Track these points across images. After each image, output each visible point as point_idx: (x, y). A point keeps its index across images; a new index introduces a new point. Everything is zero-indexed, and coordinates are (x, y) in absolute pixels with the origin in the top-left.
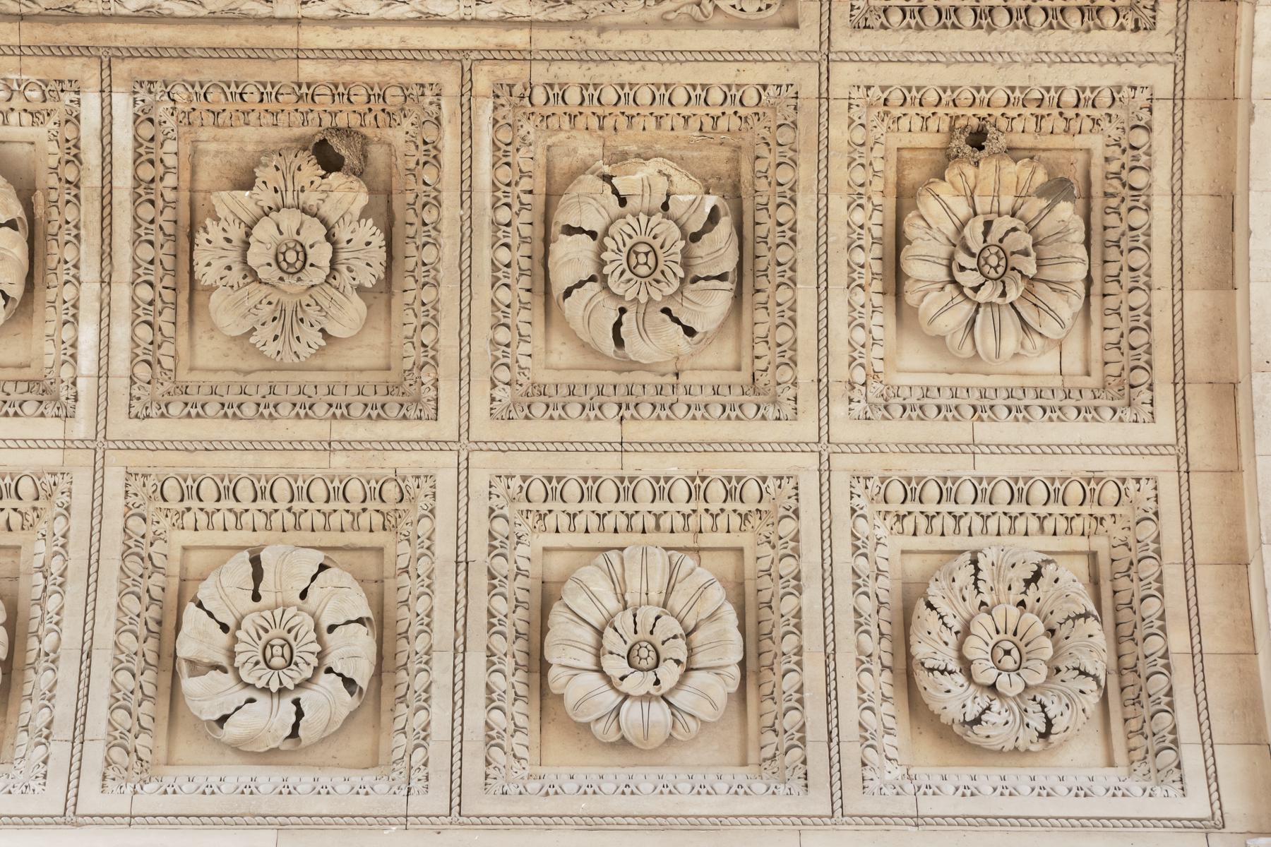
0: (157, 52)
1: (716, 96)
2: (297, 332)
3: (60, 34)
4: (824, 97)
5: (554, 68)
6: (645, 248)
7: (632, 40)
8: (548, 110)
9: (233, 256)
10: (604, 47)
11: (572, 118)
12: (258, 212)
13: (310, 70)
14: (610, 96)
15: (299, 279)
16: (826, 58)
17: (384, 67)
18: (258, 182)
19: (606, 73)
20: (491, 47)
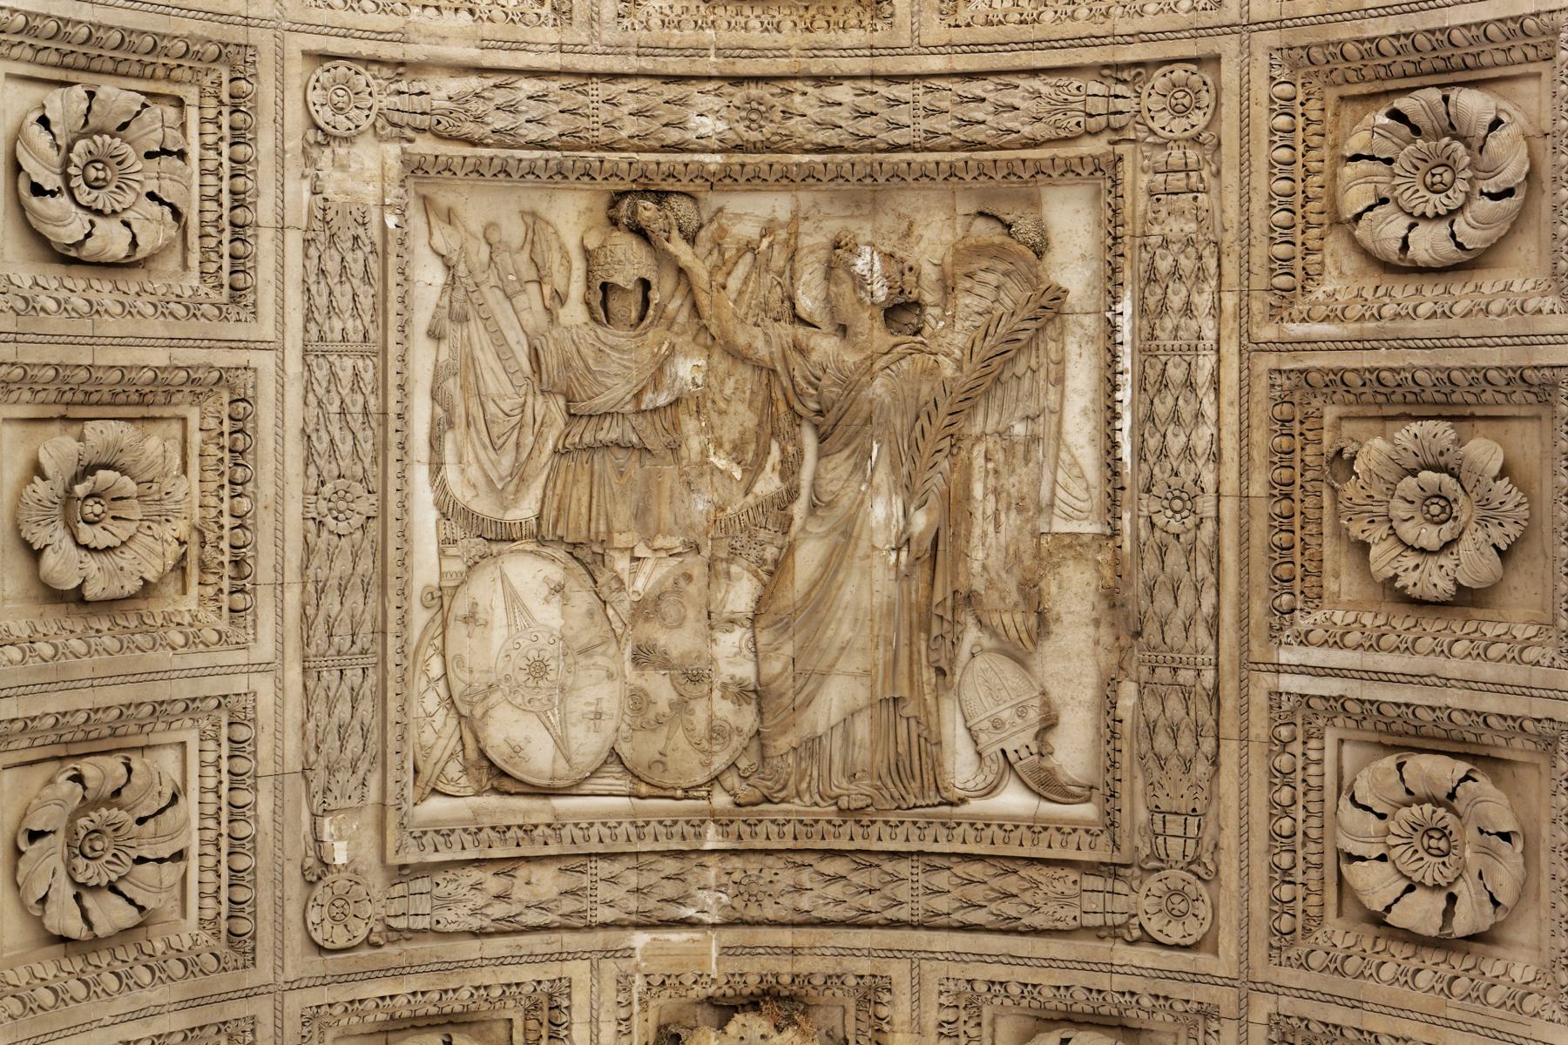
0: (1243, 620)
1: (1282, 121)
2: (1495, 504)
3: (1229, 702)
4: (1278, 24)
5: (1255, 269)
6: (1429, 179)
7: (1232, 200)
8: (1299, 273)
9: (1431, 563)
10: (1236, 225)
11: (1308, 251)
12: (1392, 539)
13: (1258, 487)
14: (1282, 217)
15: (1456, 500)
16: (1246, 27)
17: (1255, 421)
18: (1361, 537)
19: (1260, 225)
20: (1237, 326)
